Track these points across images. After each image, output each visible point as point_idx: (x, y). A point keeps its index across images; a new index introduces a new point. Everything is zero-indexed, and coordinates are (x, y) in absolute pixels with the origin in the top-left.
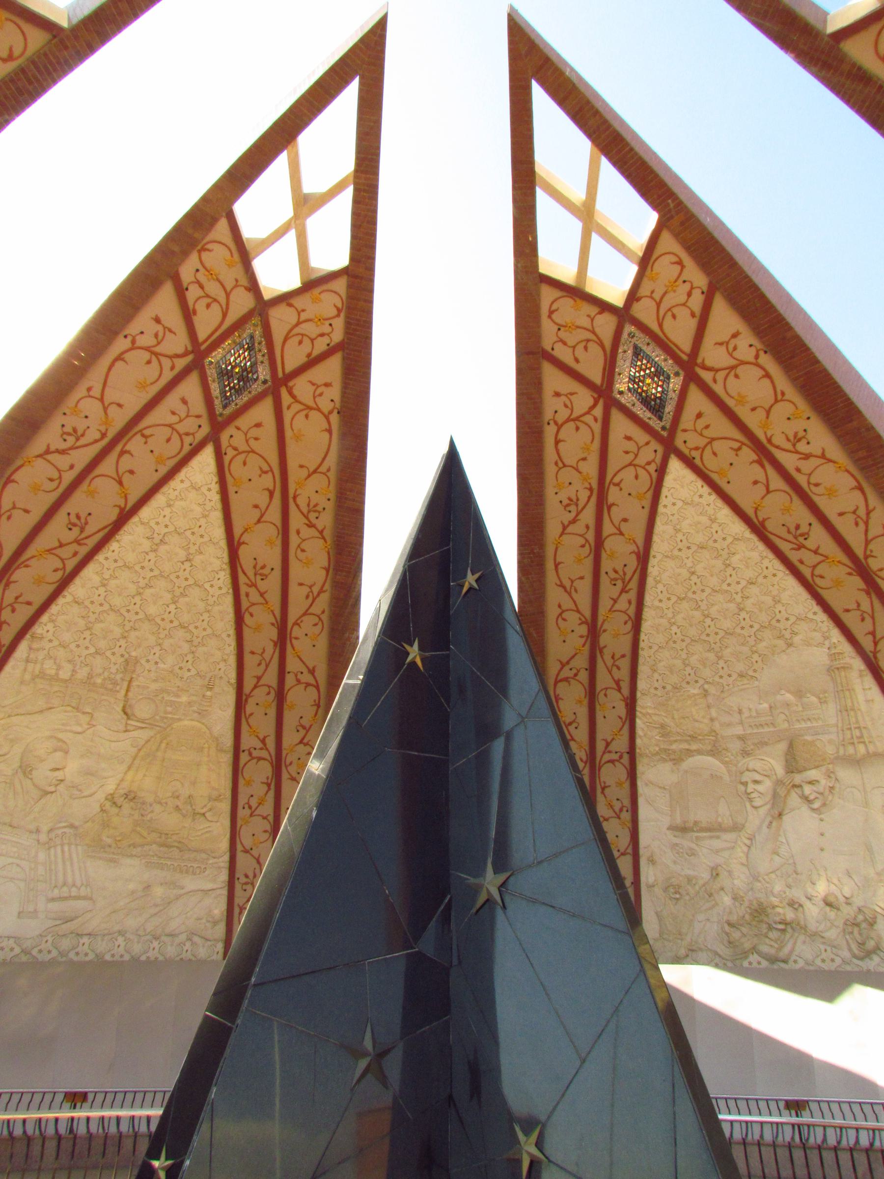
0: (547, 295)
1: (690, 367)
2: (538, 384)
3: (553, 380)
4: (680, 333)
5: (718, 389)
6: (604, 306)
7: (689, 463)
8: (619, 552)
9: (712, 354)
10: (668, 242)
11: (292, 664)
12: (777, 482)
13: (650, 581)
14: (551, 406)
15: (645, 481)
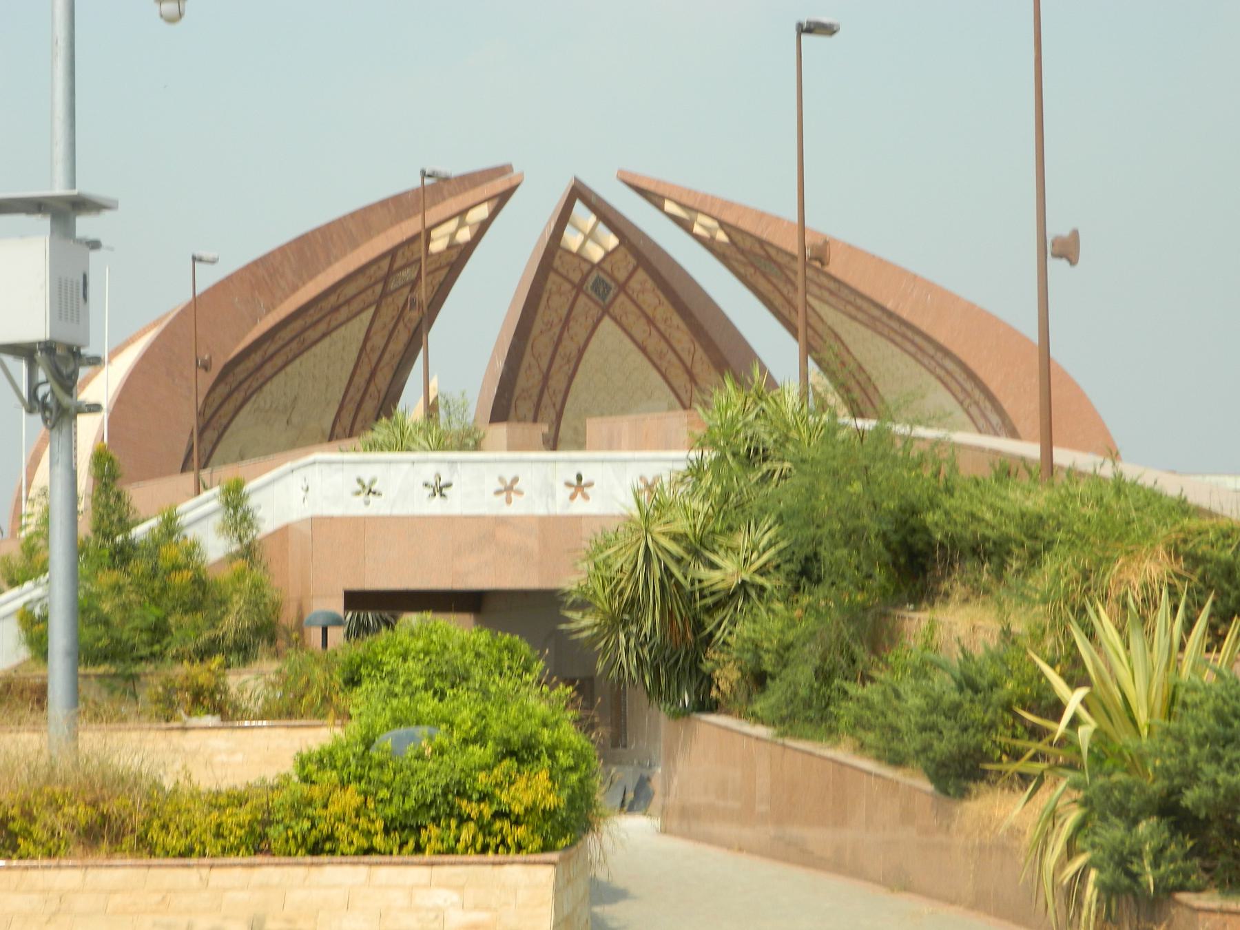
0: (559, 253)
1: (623, 287)
2: (546, 278)
3: (552, 277)
4: (621, 275)
5: (635, 296)
6: (586, 260)
7: (614, 319)
8: (569, 347)
9: (634, 284)
10: (623, 249)
11: (372, 389)
12: (654, 332)
13: (583, 362)
14: (549, 285)
15: (590, 322)
